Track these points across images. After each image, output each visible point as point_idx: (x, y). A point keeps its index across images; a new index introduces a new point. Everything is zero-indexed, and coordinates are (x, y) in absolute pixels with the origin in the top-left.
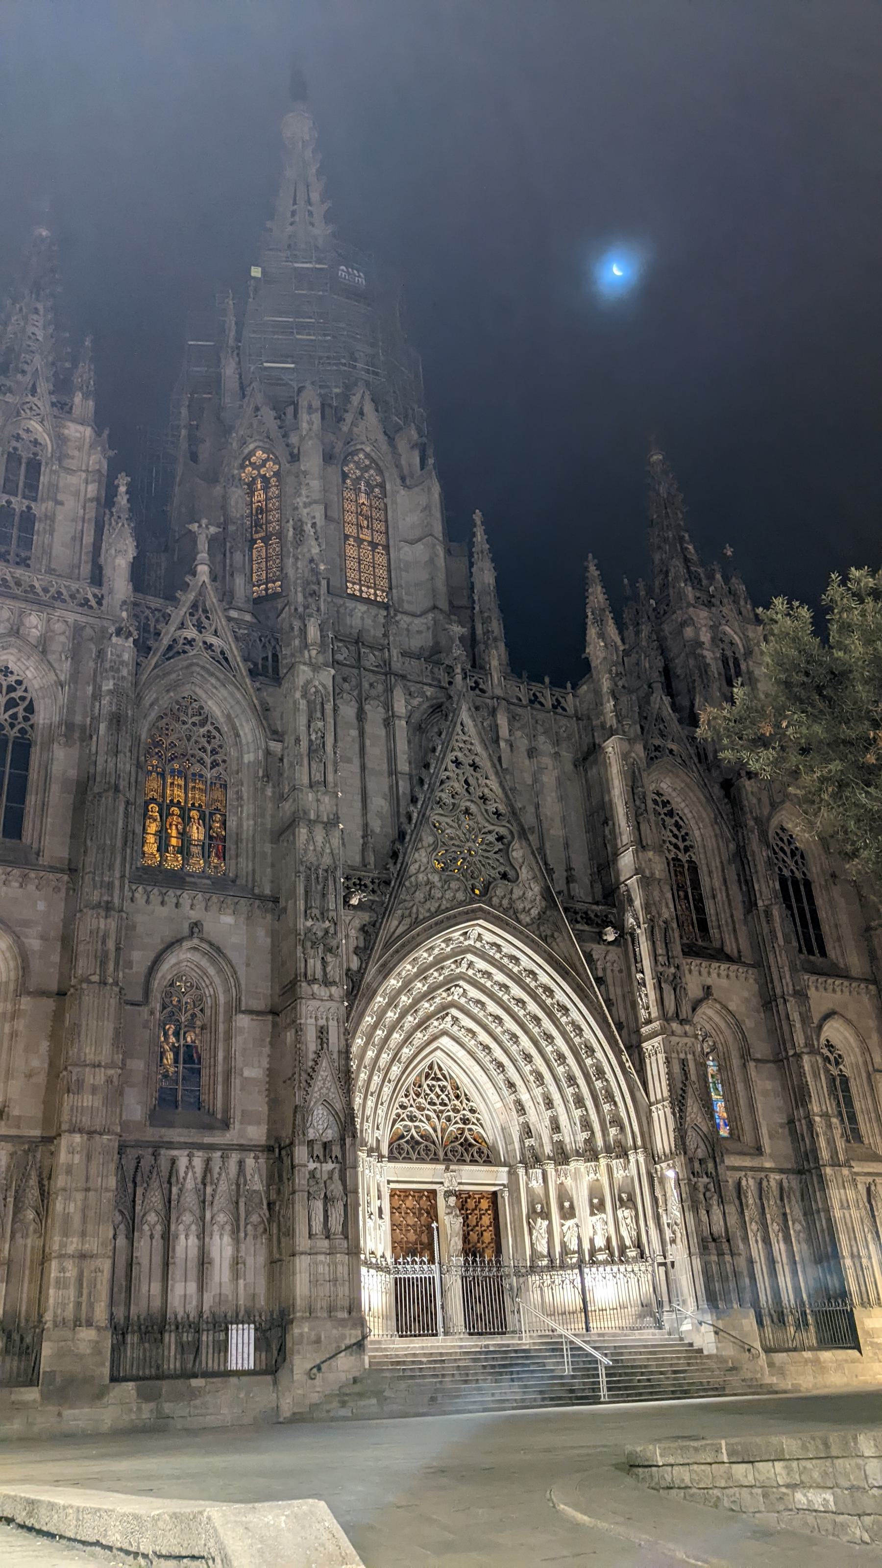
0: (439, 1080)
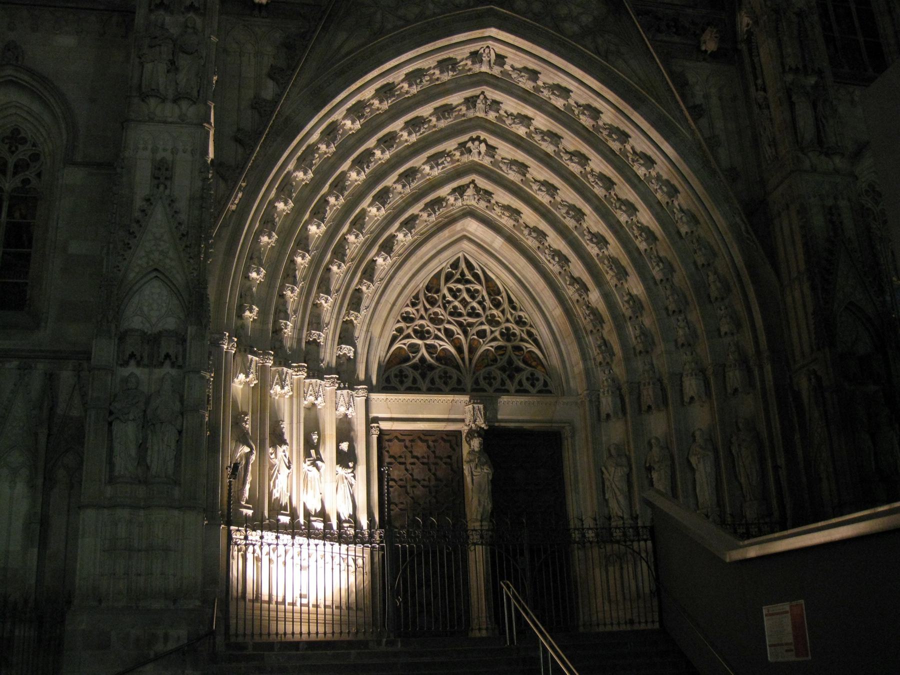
0: (468, 282)
